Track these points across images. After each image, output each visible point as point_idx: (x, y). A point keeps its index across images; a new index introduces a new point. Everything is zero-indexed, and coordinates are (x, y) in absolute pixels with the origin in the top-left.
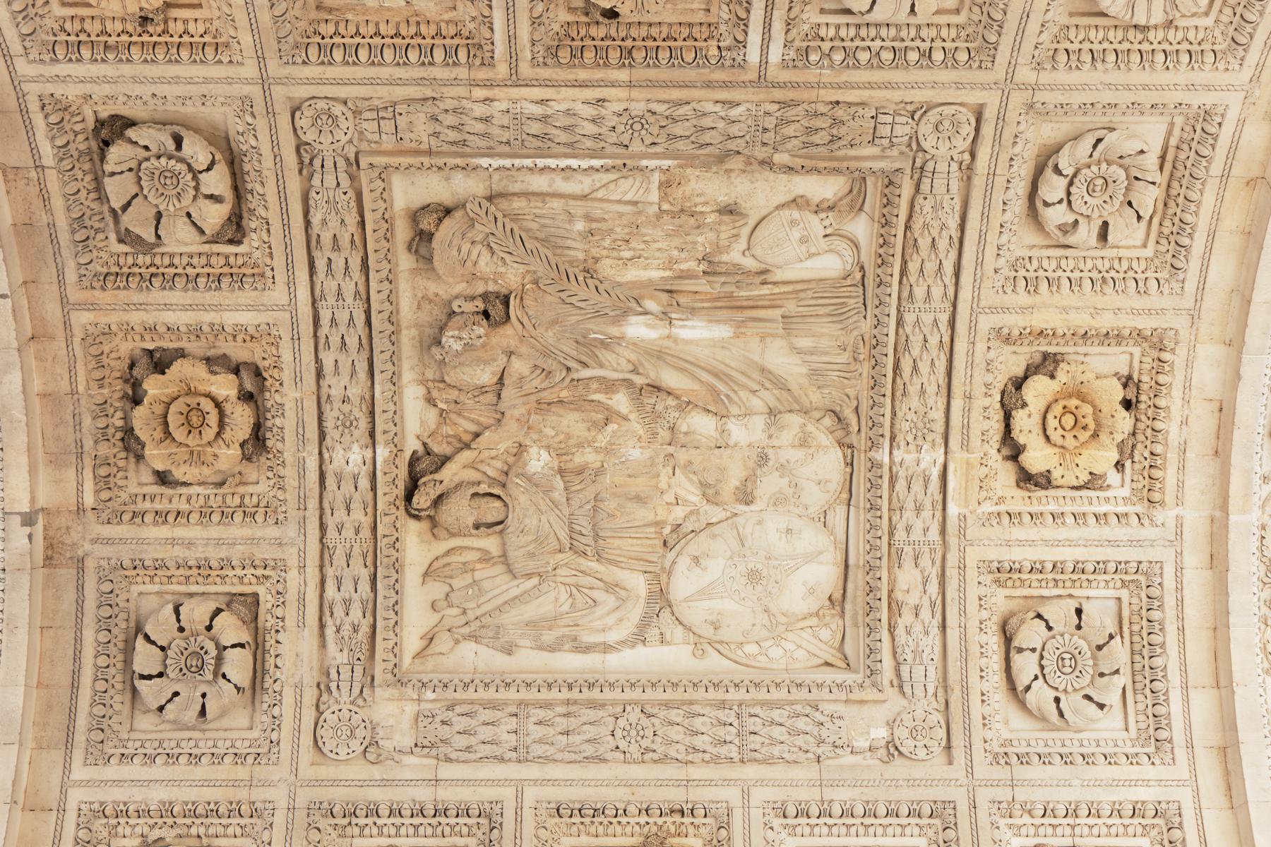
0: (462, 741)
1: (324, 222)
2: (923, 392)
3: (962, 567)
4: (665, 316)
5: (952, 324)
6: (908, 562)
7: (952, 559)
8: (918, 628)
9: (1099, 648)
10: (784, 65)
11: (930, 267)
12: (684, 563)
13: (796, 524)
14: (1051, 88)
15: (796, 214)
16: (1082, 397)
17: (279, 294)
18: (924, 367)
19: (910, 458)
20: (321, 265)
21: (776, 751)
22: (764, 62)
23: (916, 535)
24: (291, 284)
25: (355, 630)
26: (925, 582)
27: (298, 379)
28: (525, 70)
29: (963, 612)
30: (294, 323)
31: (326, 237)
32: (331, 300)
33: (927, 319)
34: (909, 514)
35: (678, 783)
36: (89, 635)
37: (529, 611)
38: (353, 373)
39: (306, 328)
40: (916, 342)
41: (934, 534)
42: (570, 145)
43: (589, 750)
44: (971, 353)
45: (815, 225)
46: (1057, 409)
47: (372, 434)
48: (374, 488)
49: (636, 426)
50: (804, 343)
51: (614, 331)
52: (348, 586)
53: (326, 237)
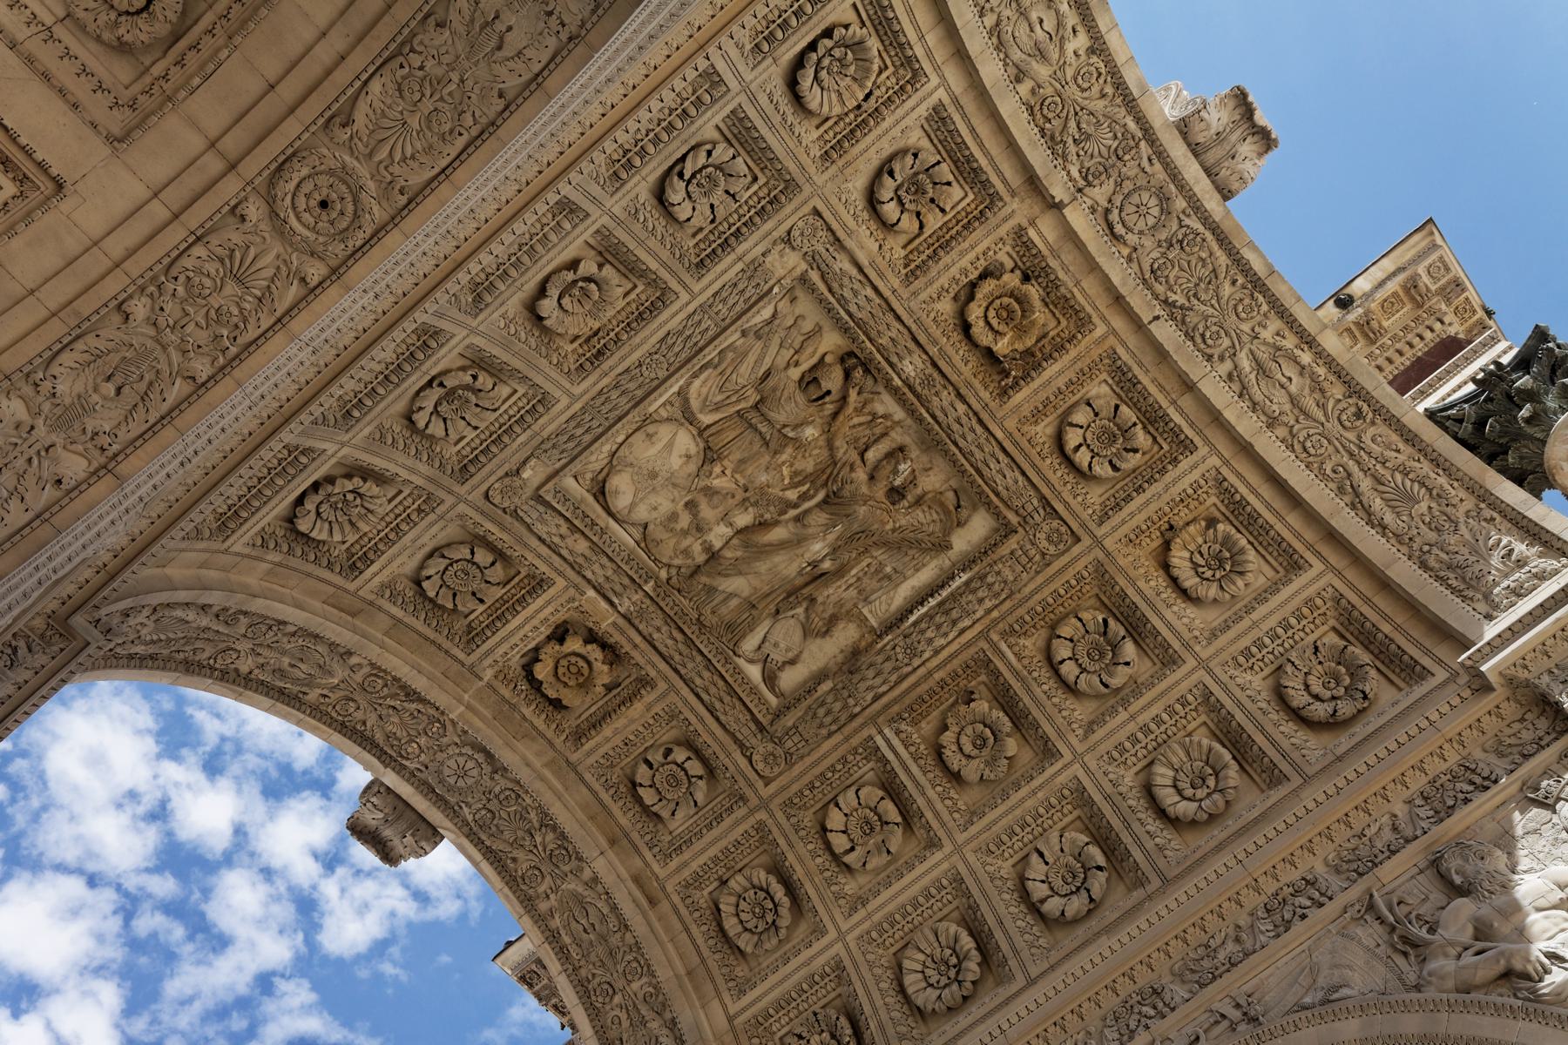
0: (741, 286)
1: (1016, 482)
2: (658, 630)
3: (561, 574)
4: (814, 564)
5: (676, 671)
6: (588, 553)
7: (570, 572)
8: (554, 531)
9: (455, 595)
10: (871, 738)
11: (713, 690)
12: (693, 450)
13: (655, 514)
14: (745, 818)
15: (790, 655)
16: (580, 686)
17: (1011, 424)
18: (670, 642)
19: (635, 597)
20: (1001, 456)
21: (573, 424)
22: (881, 732)
23: (596, 567)
24: (1010, 435)
25: (841, 286)
26: (571, 552)
27: (969, 385)
28: (983, 644)
29: (539, 556)
30: (992, 415)
31: (1008, 473)
32: (982, 441)
33: (690, 665)
34: (609, 573)
35: (612, 369)
36: (983, 162)
37: (751, 358)
38: (943, 410)
39: (985, 416)
40: (685, 650)
41: (589, 574)
42: (932, 618)
43: (670, 342)
44: (654, 666)
45: (778, 656)
46: (586, 671)
47: (910, 387)
48: (887, 360)
49: (775, 491)
50: (734, 602)
51: (831, 537)
52: (862, 302)
53: (1008, 473)
